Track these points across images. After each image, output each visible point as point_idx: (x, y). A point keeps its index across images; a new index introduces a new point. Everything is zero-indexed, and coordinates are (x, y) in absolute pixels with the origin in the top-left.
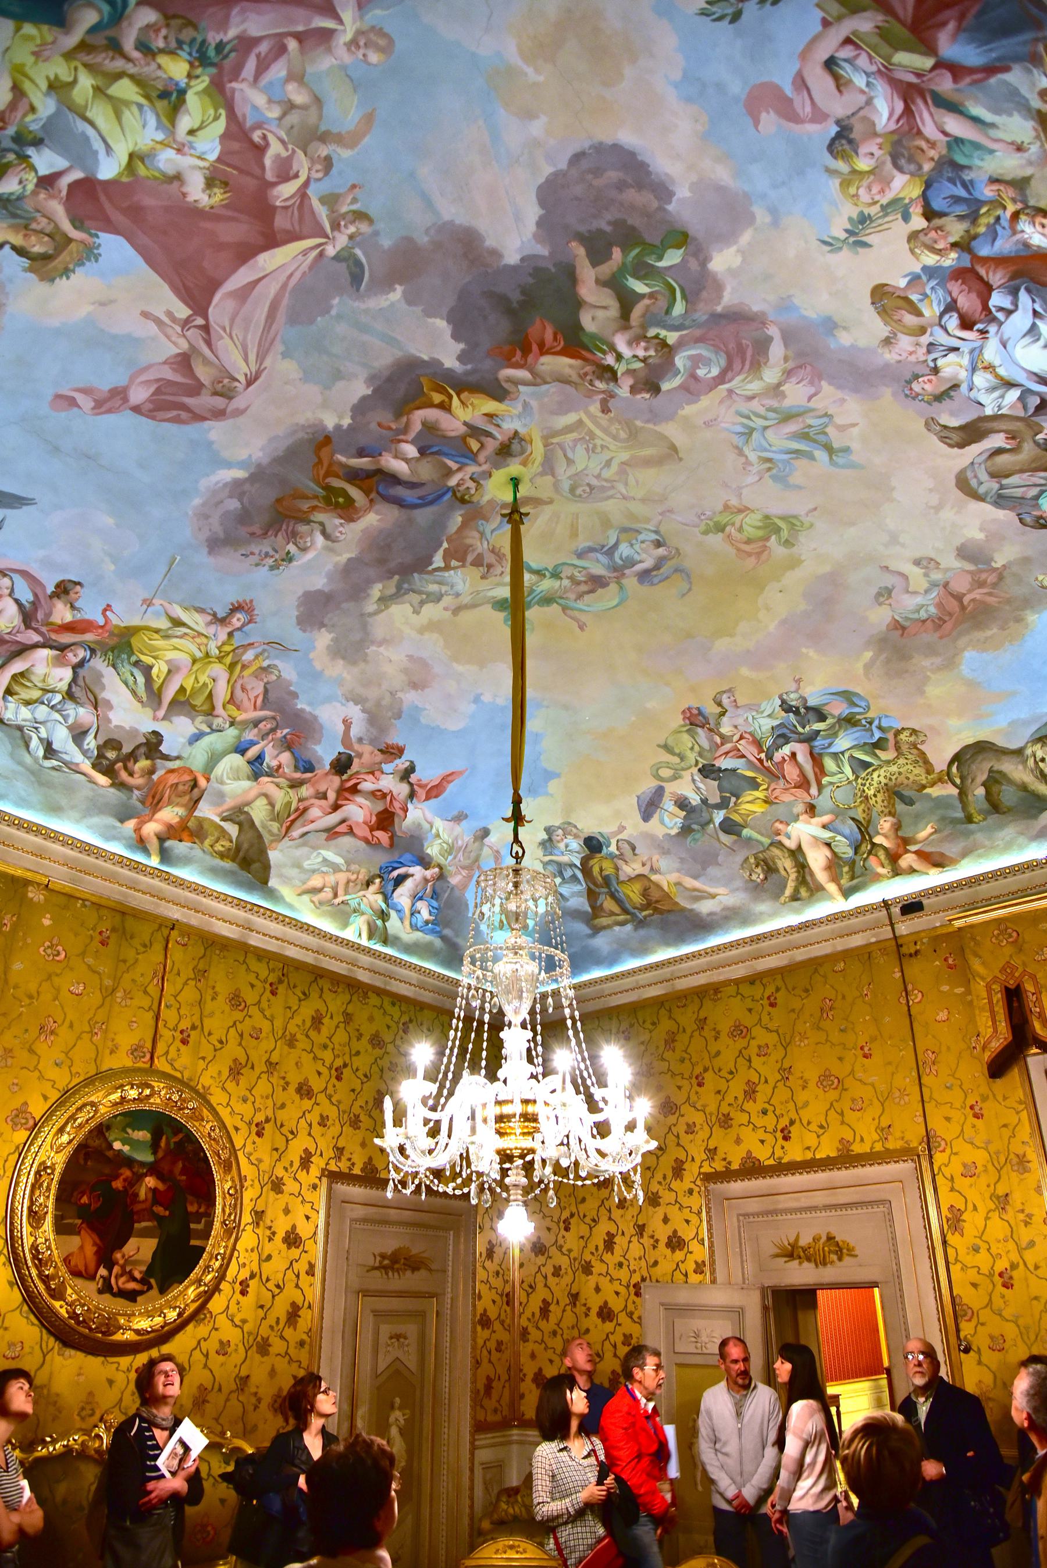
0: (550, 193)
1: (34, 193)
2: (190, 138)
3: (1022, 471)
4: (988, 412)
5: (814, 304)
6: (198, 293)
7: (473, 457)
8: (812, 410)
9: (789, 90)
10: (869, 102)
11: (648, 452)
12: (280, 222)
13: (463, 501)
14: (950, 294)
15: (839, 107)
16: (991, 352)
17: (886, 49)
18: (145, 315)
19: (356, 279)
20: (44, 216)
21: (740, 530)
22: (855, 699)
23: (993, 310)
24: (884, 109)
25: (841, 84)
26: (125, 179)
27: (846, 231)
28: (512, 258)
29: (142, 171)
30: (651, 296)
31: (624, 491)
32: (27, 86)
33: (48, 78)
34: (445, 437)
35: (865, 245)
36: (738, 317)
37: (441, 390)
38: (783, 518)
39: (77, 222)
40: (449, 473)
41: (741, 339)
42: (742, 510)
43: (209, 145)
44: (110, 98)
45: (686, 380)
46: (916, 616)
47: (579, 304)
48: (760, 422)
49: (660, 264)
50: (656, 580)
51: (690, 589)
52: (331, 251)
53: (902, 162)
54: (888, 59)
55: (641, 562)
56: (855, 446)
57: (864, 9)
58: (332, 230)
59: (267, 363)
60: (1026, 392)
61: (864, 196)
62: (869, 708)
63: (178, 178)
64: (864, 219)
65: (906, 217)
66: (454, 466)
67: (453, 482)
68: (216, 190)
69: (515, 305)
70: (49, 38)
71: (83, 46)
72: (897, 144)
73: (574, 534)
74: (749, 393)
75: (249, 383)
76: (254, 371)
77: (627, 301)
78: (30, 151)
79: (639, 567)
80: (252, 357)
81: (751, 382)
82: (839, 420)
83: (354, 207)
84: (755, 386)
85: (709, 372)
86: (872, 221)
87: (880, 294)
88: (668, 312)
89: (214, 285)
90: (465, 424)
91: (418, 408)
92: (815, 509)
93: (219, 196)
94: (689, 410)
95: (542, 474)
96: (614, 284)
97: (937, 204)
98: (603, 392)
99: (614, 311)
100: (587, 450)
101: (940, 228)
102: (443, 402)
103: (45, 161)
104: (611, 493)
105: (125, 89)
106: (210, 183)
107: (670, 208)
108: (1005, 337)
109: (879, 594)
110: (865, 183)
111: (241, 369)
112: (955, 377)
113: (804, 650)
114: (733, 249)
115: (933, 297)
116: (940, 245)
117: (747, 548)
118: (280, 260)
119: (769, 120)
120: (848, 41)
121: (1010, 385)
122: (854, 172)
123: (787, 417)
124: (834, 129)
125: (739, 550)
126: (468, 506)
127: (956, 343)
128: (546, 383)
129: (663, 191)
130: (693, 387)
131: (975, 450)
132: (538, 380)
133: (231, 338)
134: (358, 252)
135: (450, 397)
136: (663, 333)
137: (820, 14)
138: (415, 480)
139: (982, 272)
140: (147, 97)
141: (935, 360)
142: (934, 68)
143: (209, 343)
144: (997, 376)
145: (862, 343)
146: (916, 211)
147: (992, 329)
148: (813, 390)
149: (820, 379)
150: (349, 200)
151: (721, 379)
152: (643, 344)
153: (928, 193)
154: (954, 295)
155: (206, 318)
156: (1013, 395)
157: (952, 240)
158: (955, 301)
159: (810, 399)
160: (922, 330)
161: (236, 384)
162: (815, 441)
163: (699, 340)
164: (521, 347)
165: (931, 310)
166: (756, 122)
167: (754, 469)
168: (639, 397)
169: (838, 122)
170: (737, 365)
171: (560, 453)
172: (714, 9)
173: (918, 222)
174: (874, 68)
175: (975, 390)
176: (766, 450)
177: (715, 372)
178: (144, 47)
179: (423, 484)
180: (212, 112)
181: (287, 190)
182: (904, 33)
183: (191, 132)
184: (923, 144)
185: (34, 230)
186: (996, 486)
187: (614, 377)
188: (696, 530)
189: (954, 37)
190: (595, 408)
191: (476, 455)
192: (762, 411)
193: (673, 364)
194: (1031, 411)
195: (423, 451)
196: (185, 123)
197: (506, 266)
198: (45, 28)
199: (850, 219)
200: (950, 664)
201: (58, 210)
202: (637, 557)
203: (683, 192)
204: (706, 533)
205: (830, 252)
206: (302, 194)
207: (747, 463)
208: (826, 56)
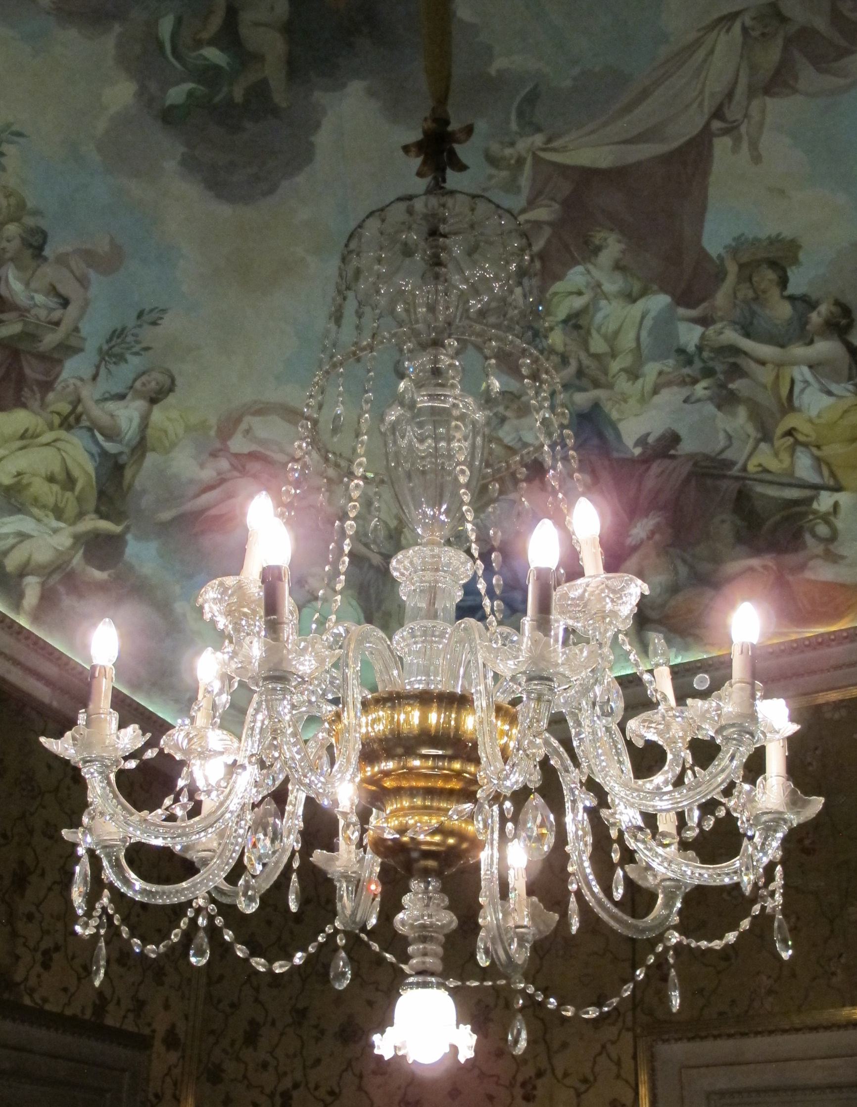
0: (301, 156)
1: (722, 319)
2: (584, 290)
6: (693, 158)
9: (92, 274)
10: (27, 284)
12: (566, 188)
15: (49, 272)
18: (757, 158)
19: (532, 99)
20: (735, 297)
25: (53, 291)
26: (655, 287)
28: (356, 88)
29: (637, 287)
30: (199, 44)
32: (649, 387)
33: (634, 383)
39: (720, 275)
43: (576, 276)
44: (612, 348)
47: (289, 29)
49: (191, 85)
52: (538, 139)
54: (26, 323)
57: (54, 349)
58: (525, 159)
59: (692, 36)
63: (618, 267)
68: (597, 242)
70: (610, 403)
71: (597, 385)
75: (733, 16)
76: (716, 32)
78: (691, 348)
80: (701, 53)
83: (493, 171)
88: (179, 21)
89: (667, 159)
93: (598, 237)
96: (244, 56)
99: (246, 17)
103: (690, 335)
105: (598, 345)
106: (598, 250)
107: (182, 149)
111: (726, 43)
118: (590, 152)
119: (103, 246)
120: (57, 324)
122: (15, 219)
124: (47, 252)
129: (190, 164)
133: (702, 92)
134: (514, 126)
140: (589, 332)
143: (730, 95)
150: (493, 181)
155: (707, 125)
161: (748, 22)
169: (45, 259)
172: (158, 315)
174: (33, 312)
178: (564, 360)
180: (555, 300)
181: (542, 214)
183: (580, 293)
185: (755, 291)
196: (578, 303)
198: (606, 410)
201: (721, 298)
203: (171, 165)
206: (532, 203)
208: (70, 308)
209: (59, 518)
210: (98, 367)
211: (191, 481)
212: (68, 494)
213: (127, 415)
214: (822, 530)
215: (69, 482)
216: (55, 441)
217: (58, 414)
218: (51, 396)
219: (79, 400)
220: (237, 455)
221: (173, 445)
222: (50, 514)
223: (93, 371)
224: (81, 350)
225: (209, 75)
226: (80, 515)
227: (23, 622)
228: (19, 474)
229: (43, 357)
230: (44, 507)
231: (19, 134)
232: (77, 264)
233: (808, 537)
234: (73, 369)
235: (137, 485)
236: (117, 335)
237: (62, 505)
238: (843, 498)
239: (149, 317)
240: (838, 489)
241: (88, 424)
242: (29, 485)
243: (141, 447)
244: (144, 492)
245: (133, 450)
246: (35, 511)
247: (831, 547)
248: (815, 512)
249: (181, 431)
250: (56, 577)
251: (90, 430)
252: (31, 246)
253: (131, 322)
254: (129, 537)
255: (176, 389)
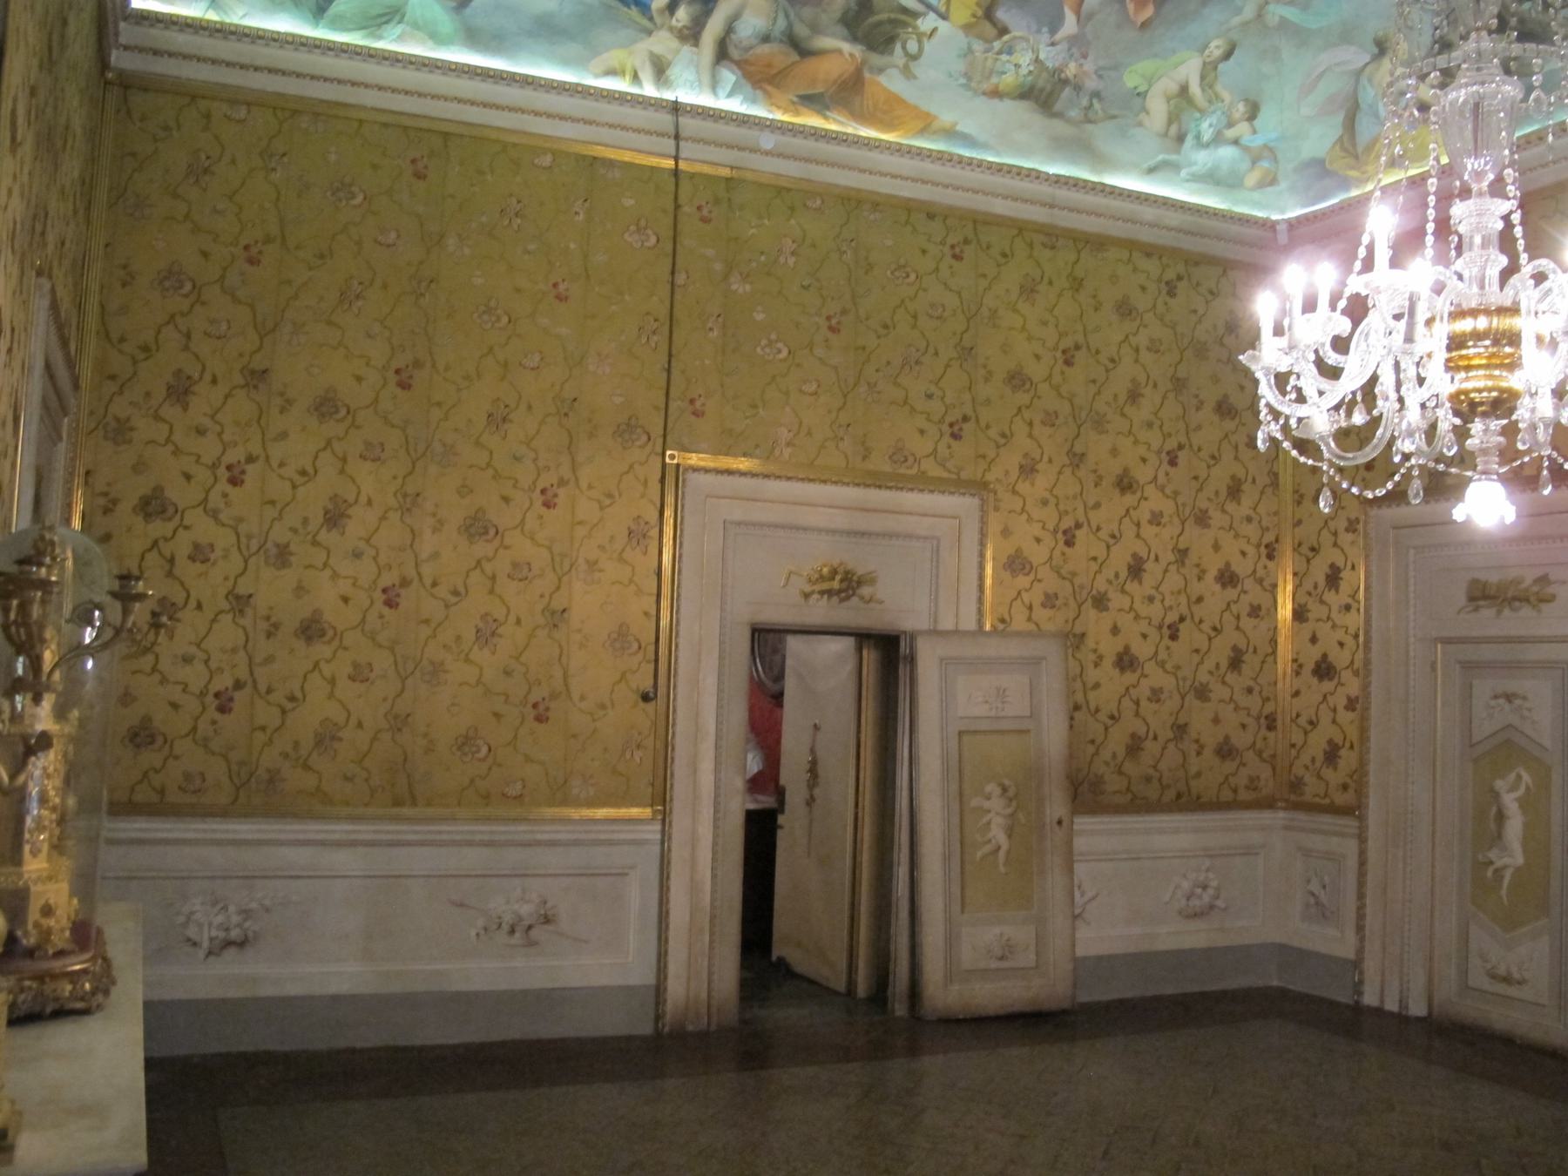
214: (912, 46)
233: (898, 47)
238: (943, 26)
240: (944, 17)
247: (912, 64)
248: (915, 27)
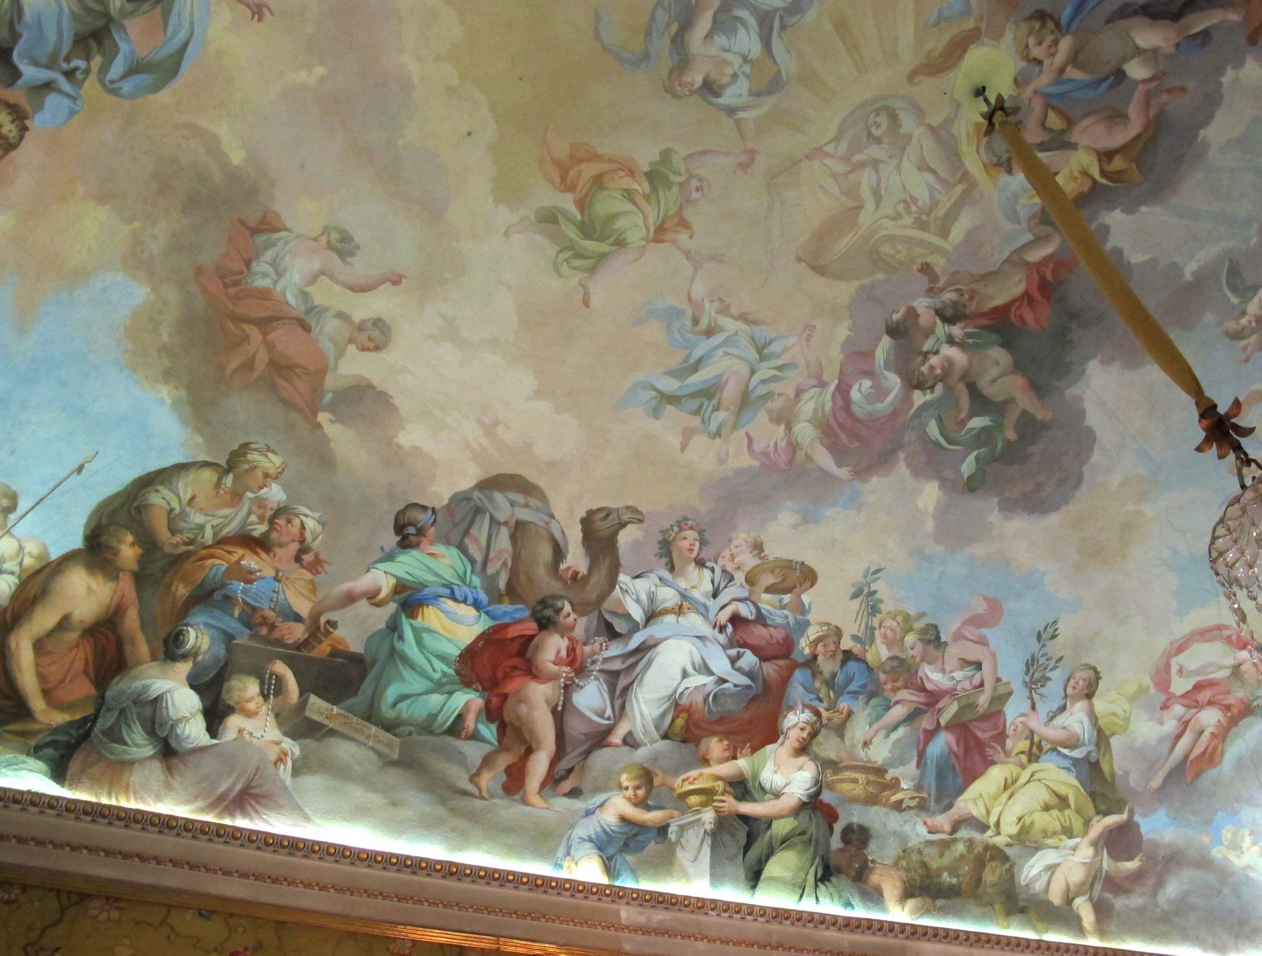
0: (1085, 440)
3: (516, 557)
4: (623, 578)
5: (837, 522)
7: (1050, 102)
8: (735, 427)
9: (984, 631)
10: (943, 671)
11: (843, 245)
13: (1041, 16)
14: (775, 627)
15: (954, 652)
16: (693, 621)
17: (964, 702)
19: (1234, 271)
21: (629, 195)
22: (145, 79)
23: (742, 650)
24: (934, 676)
25: (965, 663)
27: (875, 592)
28: (1094, 368)
30: (963, 423)
31: (828, 161)
34: (1095, 112)
35: (855, 596)
36: (880, 462)
37: (1115, 177)
38: (602, 257)
40: (1075, 59)
41: (862, 444)
42: (660, 233)
45: (874, 363)
46: (268, 255)
47: (1017, 367)
48: (765, 372)
49: (975, 453)
50: (662, 17)
51: (597, 36)
53: (895, 663)
54: (959, 699)
55: (709, 36)
56: (653, 425)
60: (635, 628)
61: (889, 623)
62: (115, 93)
64: (874, 610)
65: (855, 638)
66: (1073, 73)
67: (1065, 44)
69: (1074, 326)
72: (909, 669)
73: (841, 26)
74: (806, 396)
77: (980, 402)
79: (704, 24)
81: (815, 411)
82: (700, 441)
83: (1244, 343)
84: (807, 408)
85: (860, 391)
86: (869, 614)
87: (809, 576)
88: (940, 420)
90: (1074, 146)
91: (1138, 136)
92: (586, 303)
94: (843, 331)
95: (948, 122)
97: (852, 666)
98: (942, 290)
99: (984, 384)
100: (915, 200)
101: (834, 656)
102: (1110, 162)
104: (844, 146)
107: (996, 500)
108: (708, 643)
109: (346, 238)
110: (898, 630)
112: (682, 574)
113: (320, 71)
114: (931, 509)
115: (779, 612)
116: (820, 648)
117: (589, 170)
119: (980, 607)
120: (982, 684)
121: (652, 616)
122: (910, 630)
123: (746, 402)
124: (943, 638)
125: (595, 158)
126: (1030, 10)
127: (724, 597)
128: (1006, 261)
129: (1008, 507)
130: (858, 359)
131: (574, 536)
132: (1015, 260)
134: (1235, 300)
135: (1103, 173)
136: (929, 396)
137: (1004, 680)
138: (1122, 24)
139: (782, 662)
141: (713, 570)
142: (938, 722)
144: (666, 612)
145: (772, 527)
146: (857, 649)
147: (722, 638)
148: (758, 447)
149: (763, 465)
151: (843, 390)
152: (939, 371)
153: (864, 666)
154: (772, 630)
156: (637, 614)
157: (820, 658)
158: (765, 625)
159: (750, 440)
160: (750, 580)
162: (692, 396)
163: (895, 414)
164: (1047, 284)
165: (767, 602)
166: (986, 599)
167: (710, 309)
168: (903, 310)
169: (946, 644)
170: (841, 416)
171: (943, 173)
173: (847, 643)
174: (959, 688)
175: (658, 583)
176: (724, 344)
177: (855, 395)
179: (1107, 22)
182: (965, 719)
184: (899, 684)
186: (502, 517)
187: (939, 313)
188: (684, 153)
189: (948, 744)
190: (939, 263)
191: (1048, 106)
192: (773, 386)
193: (899, 372)
194: (608, 617)
195: (1120, 75)
197: (1094, 357)
199: (881, 601)
200: (137, 262)
202: (720, 40)
203: (995, 517)
204: (666, 155)
205: (868, 569)
207: (724, 311)
209: (1071, 837)
210: (1031, 698)
211: (1161, 740)
212: (1067, 812)
213: (1076, 720)
215: (1063, 802)
216: (1032, 775)
217: (1022, 752)
218: (1009, 743)
219: (1032, 732)
220: (1185, 696)
221: (1127, 720)
222: (1063, 837)
223: (1029, 703)
224: (1011, 693)
225: (983, 438)
226: (1087, 823)
227: (1093, 941)
228: (1020, 819)
229: (986, 717)
230: (1055, 833)
231: (878, 571)
232: (971, 632)
234: (1013, 711)
235: (1119, 772)
236: (1030, 664)
237: (1067, 824)
239: (1046, 634)
241: (1049, 746)
242: (1032, 823)
243: (1102, 738)
244: (1126, 773)
245: (1098, 745)
246: (1049, 841)
249: (1126, 706)
250: (1098, 887)
251: (1054, 750)
252: (929, 642)
253: (1034, 646)
254: (1137, 818)
255: (1102, 675)
